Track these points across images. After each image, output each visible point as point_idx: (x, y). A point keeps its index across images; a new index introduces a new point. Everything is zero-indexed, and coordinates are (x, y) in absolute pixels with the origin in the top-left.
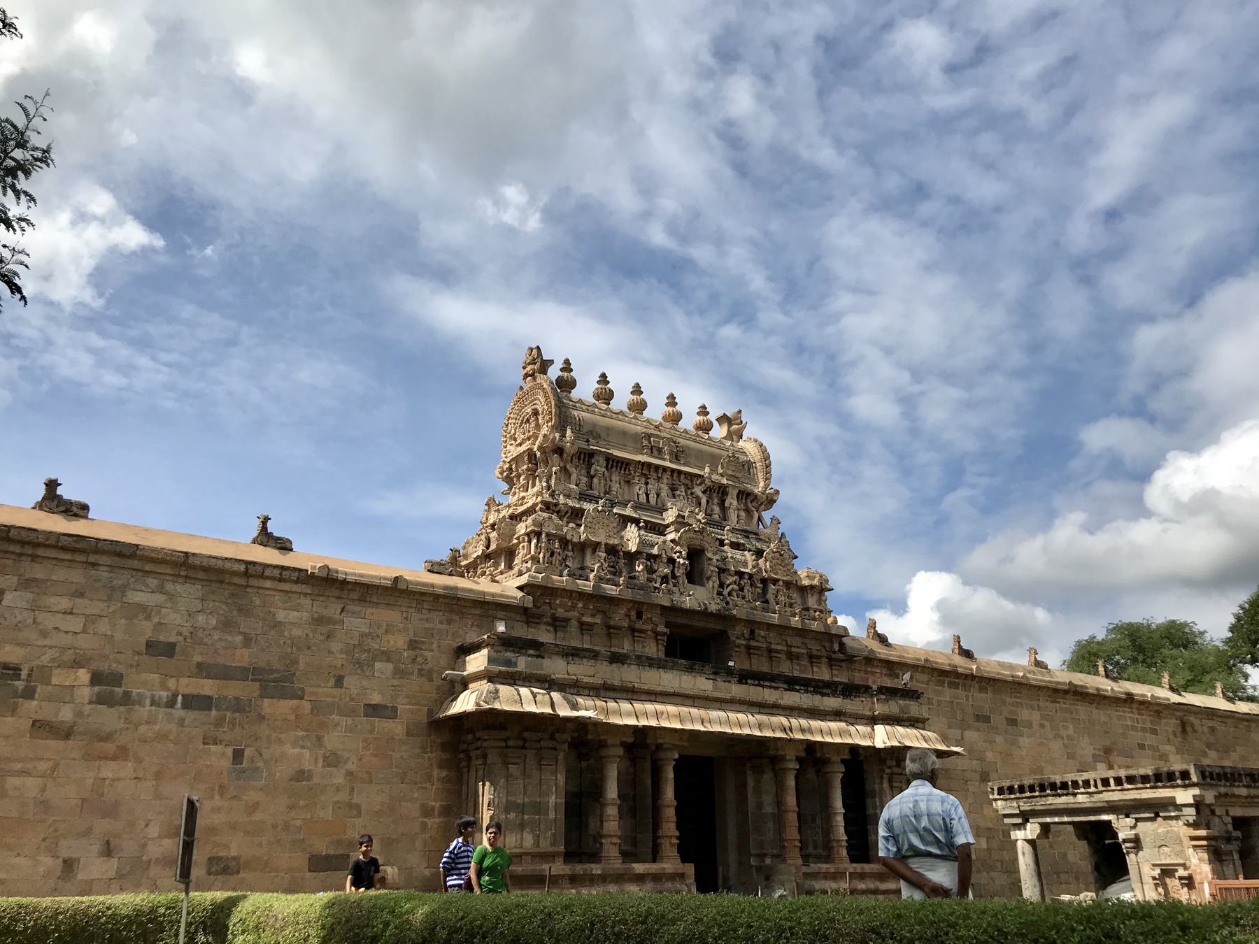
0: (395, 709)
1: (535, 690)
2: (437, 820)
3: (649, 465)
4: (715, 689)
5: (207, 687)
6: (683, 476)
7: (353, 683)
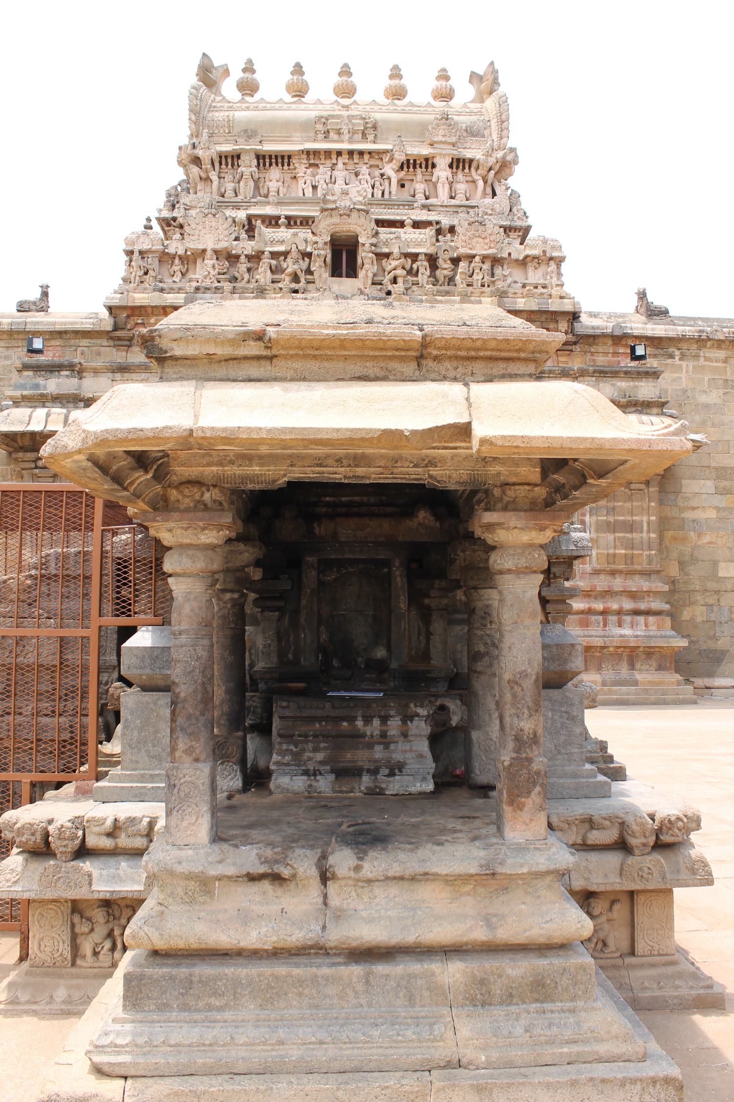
3: (316, 153)
6: (366, 157)
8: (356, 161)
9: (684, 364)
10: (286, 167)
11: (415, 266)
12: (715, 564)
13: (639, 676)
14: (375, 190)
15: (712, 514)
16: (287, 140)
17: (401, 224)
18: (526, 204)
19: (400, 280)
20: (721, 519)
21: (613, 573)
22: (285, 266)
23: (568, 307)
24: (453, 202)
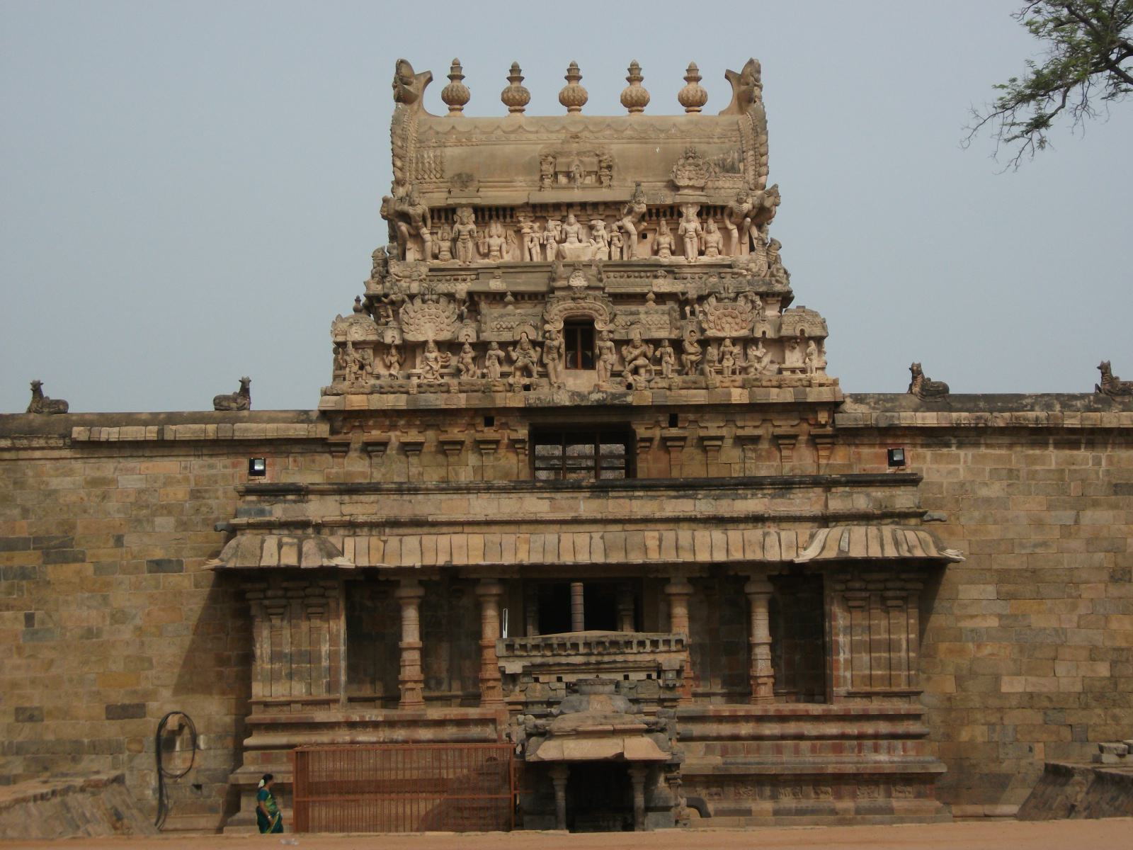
0: (180, 563)
1: (285, 540)
2: (235, 669)
4: (554, 509)
6: (601, 208)
7: (131, 540)
8: (589, 212)
9: (962, 453)
10: (508, 220)
11: (658, 354)
12: (997, 678)
13: (895, 804)
14: (613, 247)
15: (993, 622)
17: (641, 298)
18: (788, 259)
19: (642, 371)
20: (1003, 628)
21: (868, 695)
22: (515, 358)
23: (826, 395)
24: (704, 259)
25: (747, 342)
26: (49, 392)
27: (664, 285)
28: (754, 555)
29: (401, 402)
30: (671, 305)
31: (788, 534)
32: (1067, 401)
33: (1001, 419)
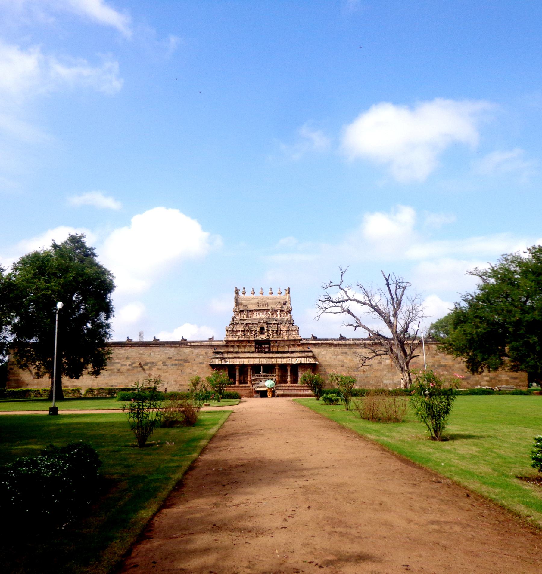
5: (176, 362)
7: (196, 360)
16: (252, 306)
18: (293, 318)
23: (299, 338)
25: (288, 330)
26: (184, 338)
27: (275, 322)
28: (288, 362)
29: (236, 339)
30: (276, 325)
31: (293, 359)
32: (335, 340)
33: (325, 342)
